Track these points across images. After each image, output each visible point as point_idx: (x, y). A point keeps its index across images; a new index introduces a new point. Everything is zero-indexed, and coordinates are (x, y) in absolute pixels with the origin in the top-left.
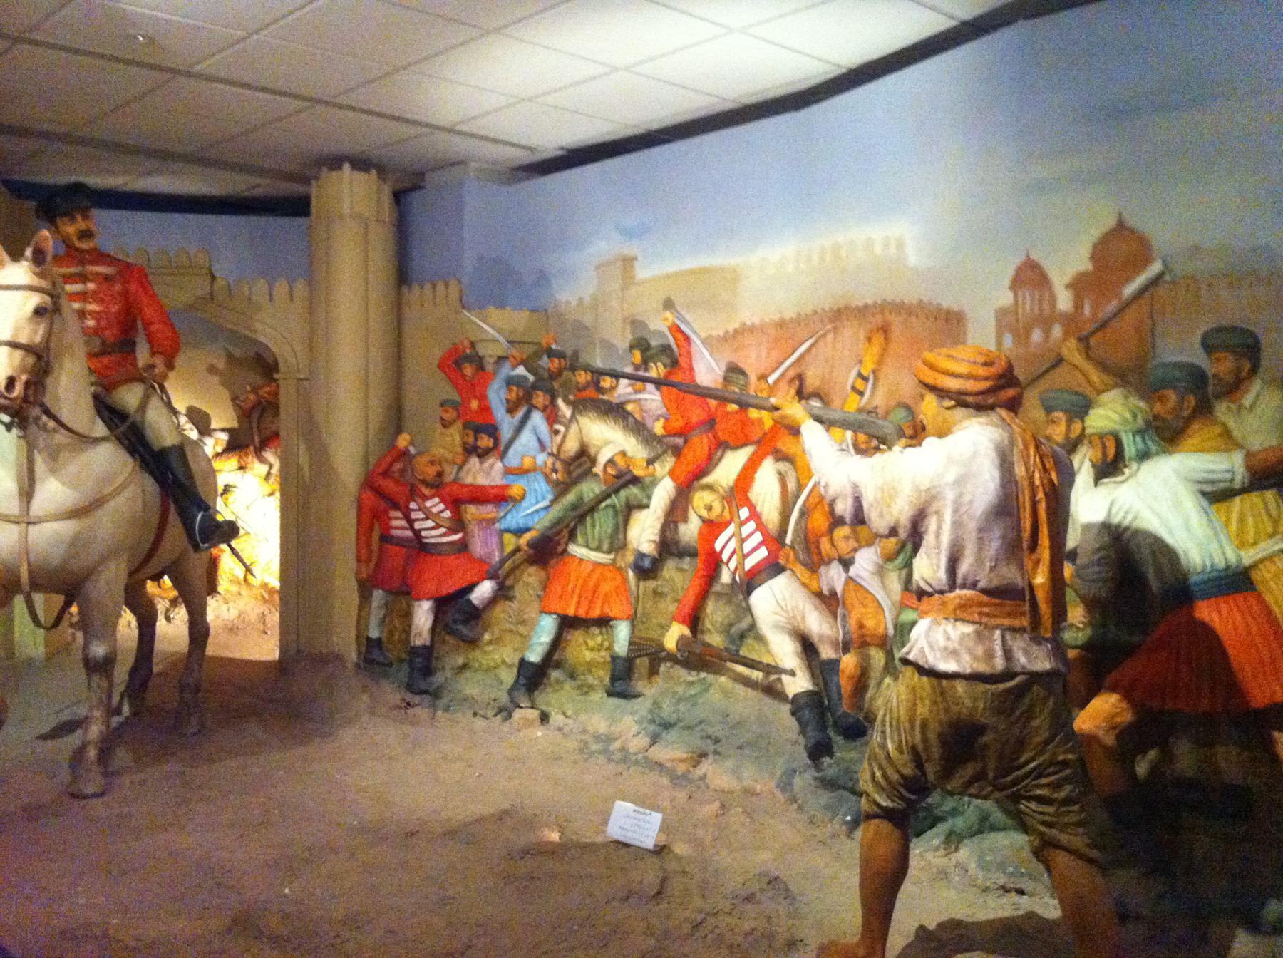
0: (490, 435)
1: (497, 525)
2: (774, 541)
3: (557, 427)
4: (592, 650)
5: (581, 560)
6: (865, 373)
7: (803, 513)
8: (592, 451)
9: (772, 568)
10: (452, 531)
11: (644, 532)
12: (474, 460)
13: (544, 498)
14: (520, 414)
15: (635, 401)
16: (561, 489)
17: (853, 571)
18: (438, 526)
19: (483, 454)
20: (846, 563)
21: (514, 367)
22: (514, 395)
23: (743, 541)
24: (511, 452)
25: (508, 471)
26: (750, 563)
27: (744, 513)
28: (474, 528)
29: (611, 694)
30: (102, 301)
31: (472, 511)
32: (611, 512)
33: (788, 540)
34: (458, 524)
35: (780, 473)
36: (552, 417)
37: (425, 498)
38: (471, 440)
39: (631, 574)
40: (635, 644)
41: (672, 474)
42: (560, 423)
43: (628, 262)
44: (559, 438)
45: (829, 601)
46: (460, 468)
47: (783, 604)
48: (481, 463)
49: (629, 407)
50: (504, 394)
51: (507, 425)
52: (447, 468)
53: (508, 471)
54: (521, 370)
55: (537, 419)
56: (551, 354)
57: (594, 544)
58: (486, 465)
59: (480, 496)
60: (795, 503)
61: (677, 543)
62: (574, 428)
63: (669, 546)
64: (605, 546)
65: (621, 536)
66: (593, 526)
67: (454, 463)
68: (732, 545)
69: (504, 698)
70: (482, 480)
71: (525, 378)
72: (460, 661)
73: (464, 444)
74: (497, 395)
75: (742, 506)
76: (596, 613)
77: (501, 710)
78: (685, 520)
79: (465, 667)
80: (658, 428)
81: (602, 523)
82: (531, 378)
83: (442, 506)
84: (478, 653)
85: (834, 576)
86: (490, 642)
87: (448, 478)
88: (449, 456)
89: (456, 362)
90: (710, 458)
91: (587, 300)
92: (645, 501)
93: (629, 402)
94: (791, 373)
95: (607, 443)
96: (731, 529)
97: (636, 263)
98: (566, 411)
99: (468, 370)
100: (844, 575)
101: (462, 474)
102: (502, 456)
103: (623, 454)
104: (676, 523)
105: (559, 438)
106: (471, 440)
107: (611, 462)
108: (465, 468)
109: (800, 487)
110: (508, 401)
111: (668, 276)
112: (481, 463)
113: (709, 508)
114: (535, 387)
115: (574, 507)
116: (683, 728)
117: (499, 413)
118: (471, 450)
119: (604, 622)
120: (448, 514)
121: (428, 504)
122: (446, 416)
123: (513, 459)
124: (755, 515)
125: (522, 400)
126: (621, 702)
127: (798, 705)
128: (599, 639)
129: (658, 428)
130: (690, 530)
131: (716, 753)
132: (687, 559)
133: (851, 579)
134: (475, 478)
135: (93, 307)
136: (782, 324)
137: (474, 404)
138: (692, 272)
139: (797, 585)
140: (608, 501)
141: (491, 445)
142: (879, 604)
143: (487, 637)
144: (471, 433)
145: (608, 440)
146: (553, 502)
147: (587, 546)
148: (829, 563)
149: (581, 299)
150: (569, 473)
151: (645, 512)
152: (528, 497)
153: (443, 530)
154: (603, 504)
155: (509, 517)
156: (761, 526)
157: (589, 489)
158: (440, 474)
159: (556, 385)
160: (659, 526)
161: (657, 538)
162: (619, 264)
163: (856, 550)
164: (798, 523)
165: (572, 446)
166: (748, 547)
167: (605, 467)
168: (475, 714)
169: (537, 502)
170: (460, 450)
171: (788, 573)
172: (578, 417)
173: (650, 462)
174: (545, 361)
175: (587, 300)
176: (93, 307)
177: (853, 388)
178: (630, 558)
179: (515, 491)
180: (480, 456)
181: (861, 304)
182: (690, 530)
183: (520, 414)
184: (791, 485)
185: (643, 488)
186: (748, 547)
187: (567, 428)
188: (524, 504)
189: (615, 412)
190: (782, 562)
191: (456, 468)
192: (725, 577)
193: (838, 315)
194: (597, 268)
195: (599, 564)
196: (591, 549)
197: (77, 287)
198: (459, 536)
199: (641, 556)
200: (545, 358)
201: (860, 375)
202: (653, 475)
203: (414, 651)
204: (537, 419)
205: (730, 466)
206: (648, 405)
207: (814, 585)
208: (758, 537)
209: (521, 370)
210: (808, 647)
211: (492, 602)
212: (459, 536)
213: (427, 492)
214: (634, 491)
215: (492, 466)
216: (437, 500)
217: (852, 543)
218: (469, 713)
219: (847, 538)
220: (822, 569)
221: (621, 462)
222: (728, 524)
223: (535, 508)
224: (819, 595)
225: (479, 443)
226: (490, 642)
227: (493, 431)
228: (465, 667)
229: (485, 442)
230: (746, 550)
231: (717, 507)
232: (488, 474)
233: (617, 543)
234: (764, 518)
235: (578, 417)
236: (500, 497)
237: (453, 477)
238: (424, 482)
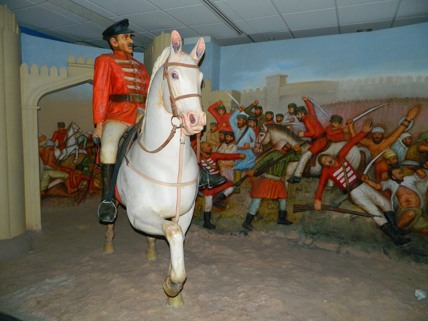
0: (231, 136)
1: (234, 168)
2: (358, 172)
3: (261, 133)
4: (268, 209)
5: (271, 179)
6: (409, 119)
7: (374, 163)
8: (274, 142)
9: (358, 182)
10: (216, 170)
11: (296, 168)
12: (224, 145)
13: (252, 158)
14: (244, 129)
15: (291, 125)
16: (258, 155)
17: (402, 184)
18: (212, 168)
19: (228, 143)
20: (399, 181)
21: (241, 112)
22: (241, 122)
23: (347, 173)
24: (240, 142)
25: (239, 149)
26: (350, 180)
27: (346, 164)
28: (223, 169)
29: (279, 223)
30: (140, 78)
31: (223, 163)
32: (284, 163)
33: (365, 173)
34: (218, 168)
35: (361, 152)
36: (258, 131)
37: (207, 159)
38: (223, 137)
39: (287, 183)
40: (296, 207)
41: (309, 150)
42: (262, 132)
43: (283, 78)
44: (263, 138)
45: (387, 194)
46: (219, 147)
47: (367, 194)
48: (228, 146)
49: (288, 127)
50: (236, 121)
51: (238, 132)
52: (214, 148)
53: (239, 149)
54: (243, 113)
55: (251, 131)
56: (256, 107)
57: (276, 174)
58: (230, 146)
59: (227, 157)
60: (370, 161)
61: (309, 173)
62: (268, 134)
63: (306, 174)
64: (280, 175)
65: (285, 171)
66: (277, 168)
67: (216, 146)
68: (343, 174)
69: (242, 229)
70: (228, 152)
71: (246, 116)
72: (219, 216)
73: (220, 139)
74: (233, 121)
75: (345, 162)
76: (276, 197)
77: (241, 232)
78: (314, 165)
79: (220, 218)
80: (301, 134)
81: (280, 167)
82: (248, 116)
83: (212, 161)
84: (224, 212)
85: (394, 186)
86: (229, 209)
87: (214, 151)
88: (214, 143)
89: (216, 109)
90: (326, 145)
91: (261, 89)
92: (296, 159)
93: (288, 125)
94: (364, 118)
95: (282, 140)
96: (341, 169)
97: (287, 78)
98: (266, 129)
99: (221, 112)
100: (397, 185)
101: (219, 150)
102: (237, 144)
103: (288, 143)
104: (310, 167)
105: (263, 138)
106: (223, 137)
107: (285, 146)
108: (221, 147)
109: (372, 157)
110: (238, 124)
111: (303, 83)
112: (228, 146)
113: (331, 162)
114: (249, 119)
115: (268, 161)
116: (322, 234)
117: (234, 128)
118: (223, 141)
119: (277, 200)
120: (214, 164)
121: (208, 160)
122: (213, 129)
123: (241, 144)
124: (349, 165)
125: (244, 124)
126: (285, 226)
127: (381, 228)
128: (273, 206)
129: (301, 134)
130: (316, 168)
131: (345, 243)
132: (311, 178)
133: (404, 187)
134: (225, 151)
135: (138, 80)
136: (358, 102)
137: (224, 125)
138: (315, 82)
139: (369, 187)
140: (283, 160)
141: (232, 139)
142: (417, 194)
143: (228, 206)
144: (223, 135)
145: (280, 138)
146: (256, 159)
147: (273, 174)
148: (386, 180)
149: (258, 89)
150: (263, 149)
151: (295, 164)
152: (246, 159)
153: (213, 170)
154: (281, 161)
155: (239, 165)
156: (352, 168)
157: (276, 156)
158: (211, 150)
159: (258, 119)
160: (304, 167)
161: (302, 172)
162: (279, 77)
163: (403, 177)
164: (371, 167)
165: (267, 140)
166: (349, 175)
167: (283, 148)
168: (231, 234)
169: (250, 160)
170: (218, 141)
171: (364, 183)
172: (271, 131)
173: (301, 146)
174: (253, 110)
175: (261, 89)
176: (138, 80)
177: (402, 124)
178: (287, 178)
179: (242, 156)
180: (227, 143)
181: (404, 97)
182: (316, 168)
183: (244, 129)
184: (368, 154)
185: (296, 155)
186: (349, 175)
187: (266, 134)
188: (246, 160)
189: (282, 128)
190: (363, 179)
191: (217, 147)
192: (331, 183)
193: (390, 101)
194: (267, 78)
195: (276, 181)
196: (275, 176)
197: (131, 70)
198: (217, 172)
199: (297, 178)
200: (254, 109)
201: (406, 120)
202: (300, 151)
203: (205, 214)
204: (251, 131)
205: (335, 148)
206: (295, 127)
207: (378, 187)
208: (352, 172)
209: (243, 113)
210: (380, 208)
211: (230, 195)
212: (217, 172)
213: (207, 156)
214: (292, 156)
215: (232, 147)
216: (210, 159)
217: (402, 175)
218: (229, 233)
219: (400, 173)
220: (382, 182)
221: (288, 146)
222: (339, 168)
223: (249, 162)
224: (380, 191)
225: (227, 138)
226: (229, 209)
227: (232, 134)
228: (220, 218)
229: (229, 138)
230: (348, 176)
231: (333, 162)
232: (231, 150)
233: (284, 173)
234: (353, 165)
235: (271, 131)
236: (235, 157)
237: (216, 150)
238: (206, 153)
